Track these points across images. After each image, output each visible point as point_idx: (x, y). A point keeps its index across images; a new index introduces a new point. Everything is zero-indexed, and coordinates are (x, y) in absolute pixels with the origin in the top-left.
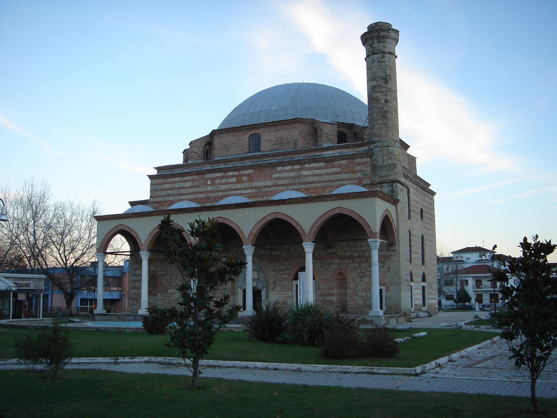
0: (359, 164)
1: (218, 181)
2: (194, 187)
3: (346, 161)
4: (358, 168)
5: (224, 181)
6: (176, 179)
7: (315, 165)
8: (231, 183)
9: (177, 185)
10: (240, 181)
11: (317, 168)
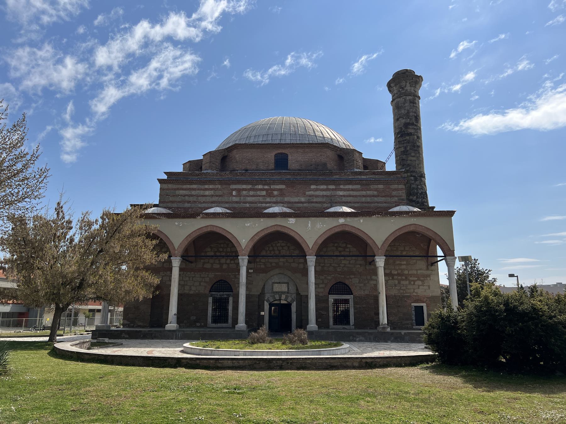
2: (217, 196)
3: (382, 186)
4: (394, 193)
5: (251, 193)
6: (195, 186)
7: (350, 187)
8: (260, 196)
9: (193, 193)
10: (270, 193)
11: (352, 190)
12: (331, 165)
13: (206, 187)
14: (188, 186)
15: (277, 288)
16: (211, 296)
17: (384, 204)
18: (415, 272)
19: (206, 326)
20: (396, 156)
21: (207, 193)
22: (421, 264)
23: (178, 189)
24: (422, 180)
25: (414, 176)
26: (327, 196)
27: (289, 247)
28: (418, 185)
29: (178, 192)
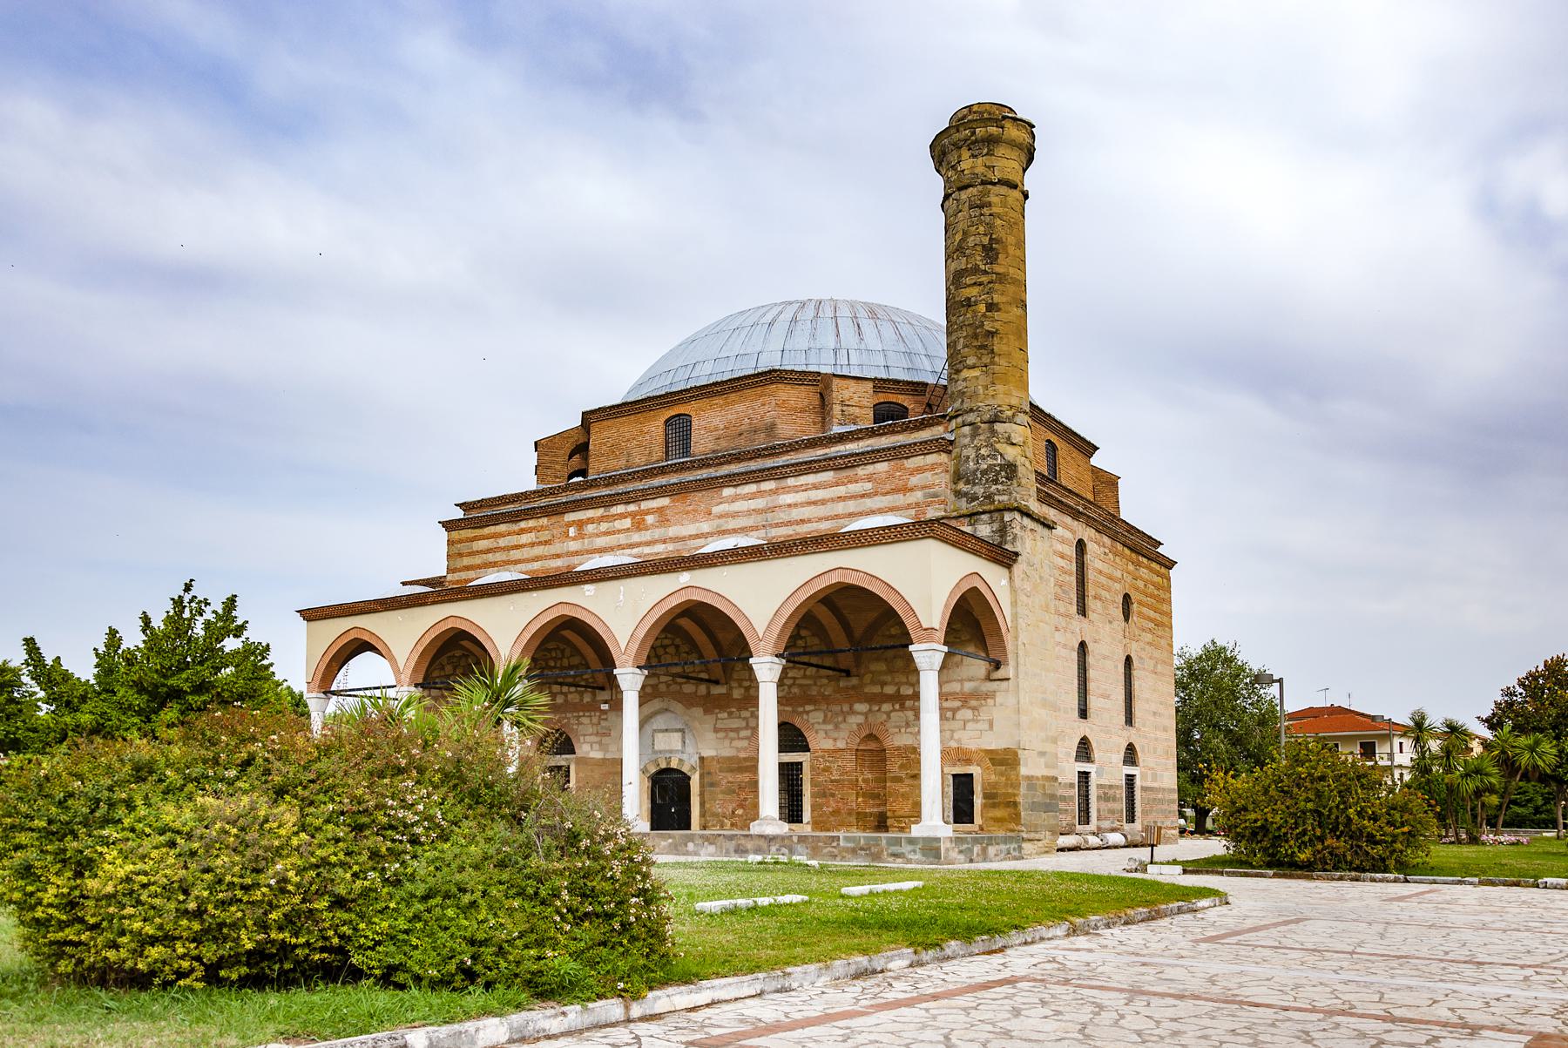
1: (590, 528)
5: (604, 526)
8: (619, 531)
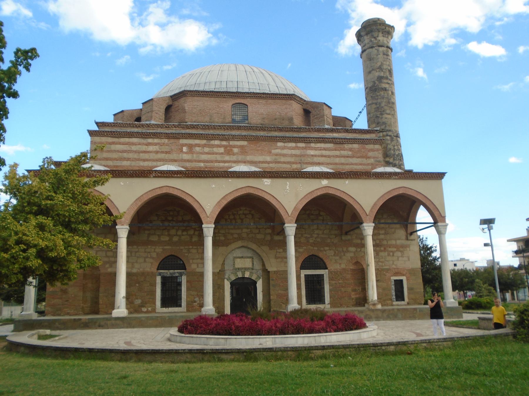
0: (372, 150)
1: (198, 149)
2: (162, 152)
5: (206, 150)
7: (322, 145)
8: (216, 154)
9: (134, 148)
10: (229, 151)
11: (325, 149)
12: (298, 121)
13: (150, 140)
14: (127, 140)
15: (239, 263)
16: (160, 274)
17: (360, 166)
18: (393, 242)
19: (154, 310)
20: (368, 113)
21: (151, 148)
22: (402, 233)
23: (113, 143)
24: (398, 140)
25: (390, 136)
26: (296, 156)
27: (253, 215)
28: (394, 146)
29: (113, 147)
